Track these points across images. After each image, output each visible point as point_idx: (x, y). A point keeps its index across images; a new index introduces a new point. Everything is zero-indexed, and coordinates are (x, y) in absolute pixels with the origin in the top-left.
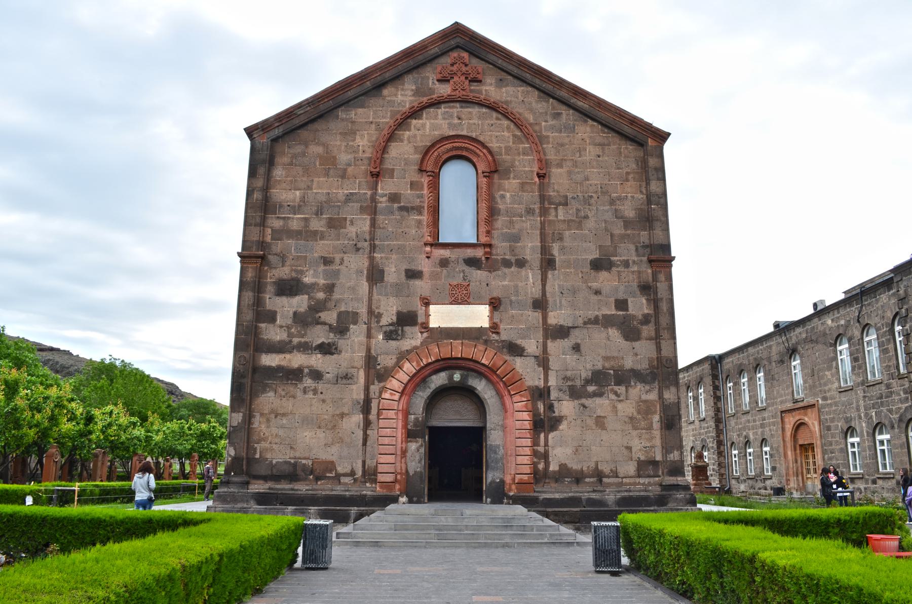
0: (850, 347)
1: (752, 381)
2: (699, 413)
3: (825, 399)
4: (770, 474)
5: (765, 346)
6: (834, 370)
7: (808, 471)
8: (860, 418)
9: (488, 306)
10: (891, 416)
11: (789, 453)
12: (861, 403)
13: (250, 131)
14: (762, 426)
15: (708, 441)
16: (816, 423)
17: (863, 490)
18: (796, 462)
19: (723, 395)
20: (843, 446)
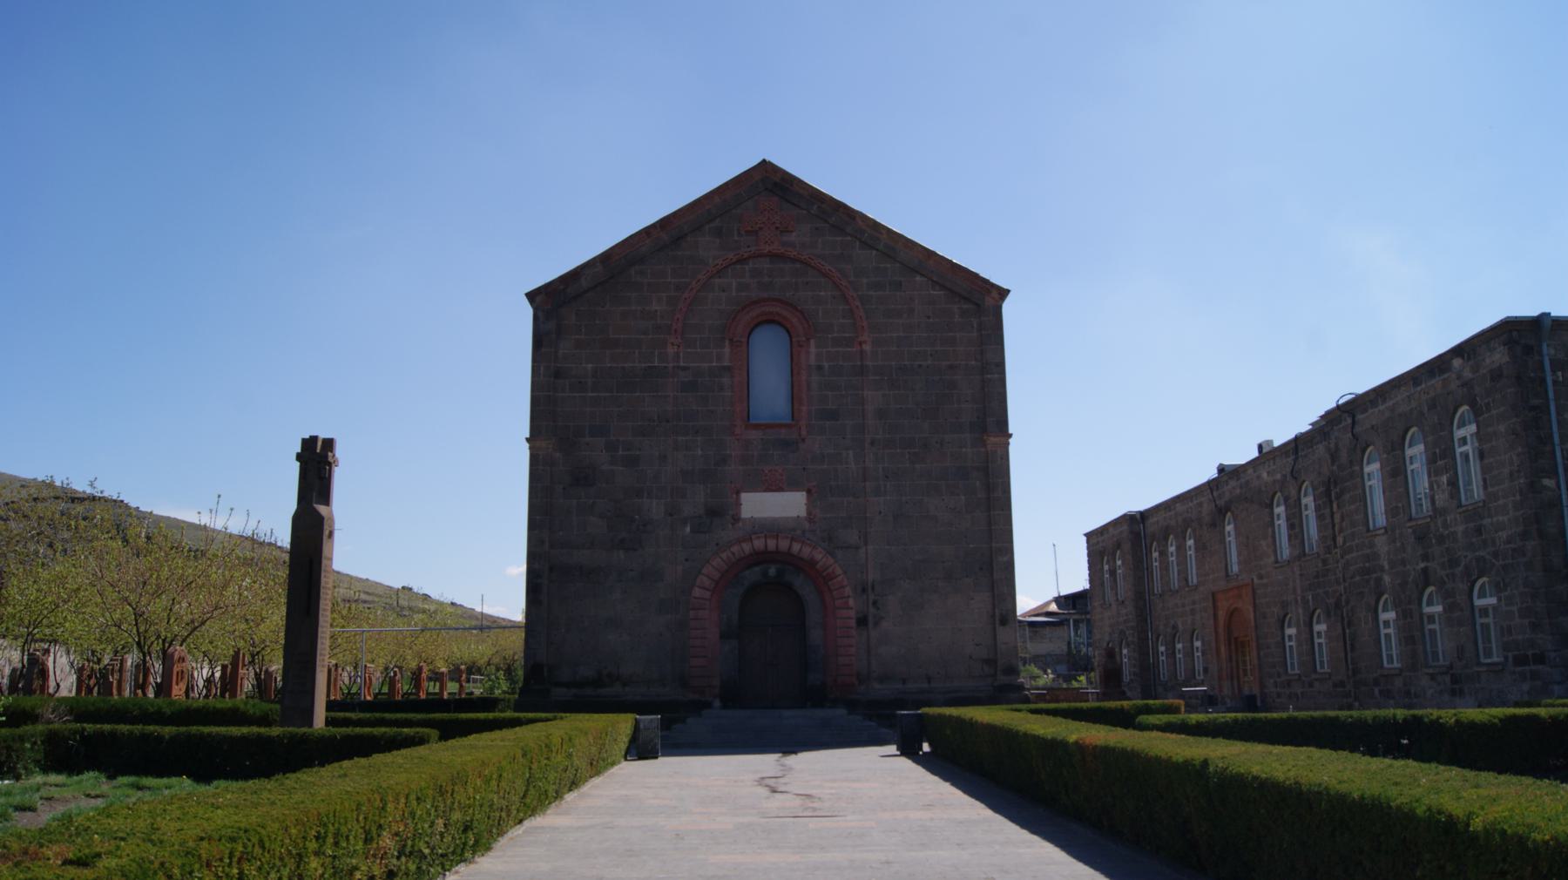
0: (1286, 510)
1: (1181, 548)
2: (1117, 594)
3: (1260, 577)
4: (1202, 677)
5: (1195, 502)
6: (1270, 540)
7: (1245, 671)
8: (1297, 601)
9: (804, 493)
10: (1327, 601)
11: (1223, 649)
12: (1298, 581)
13: (532, 296)
14: (1193, 612)
15: (1127, 633)
16: (1251, 609)
17: (1300, 696)
18: (1231, 660)
19: (1147, 569)
20: (1279, 639)
